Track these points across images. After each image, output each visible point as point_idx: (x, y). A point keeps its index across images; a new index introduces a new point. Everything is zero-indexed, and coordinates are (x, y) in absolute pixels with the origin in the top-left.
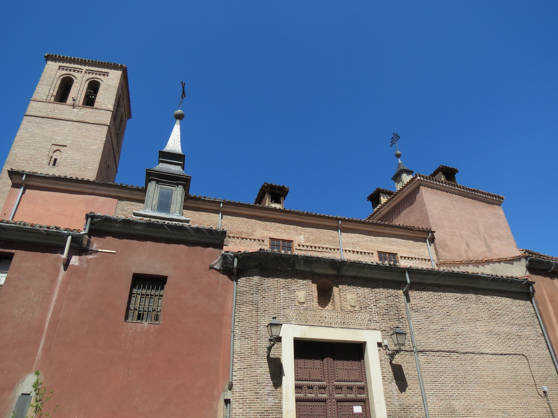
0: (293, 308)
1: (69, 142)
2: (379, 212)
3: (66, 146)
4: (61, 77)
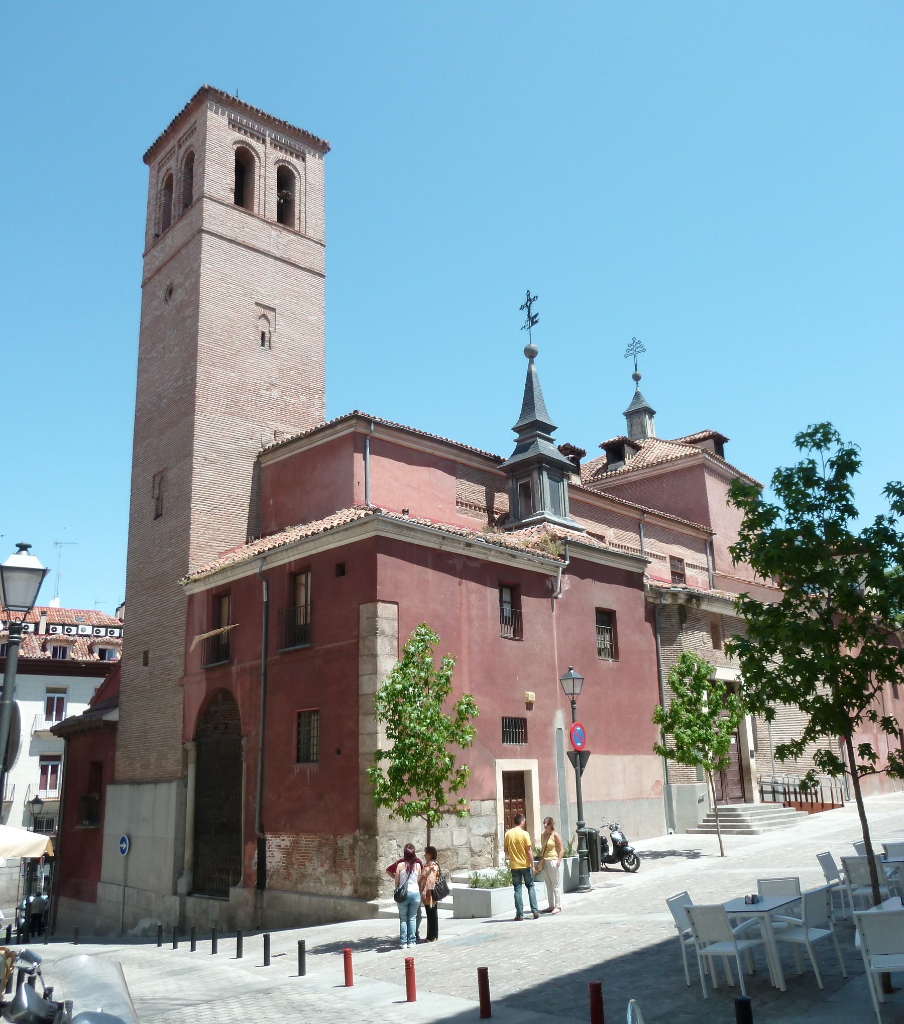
1: (277, 301)
2: (625, 476)
4: (235, 147)
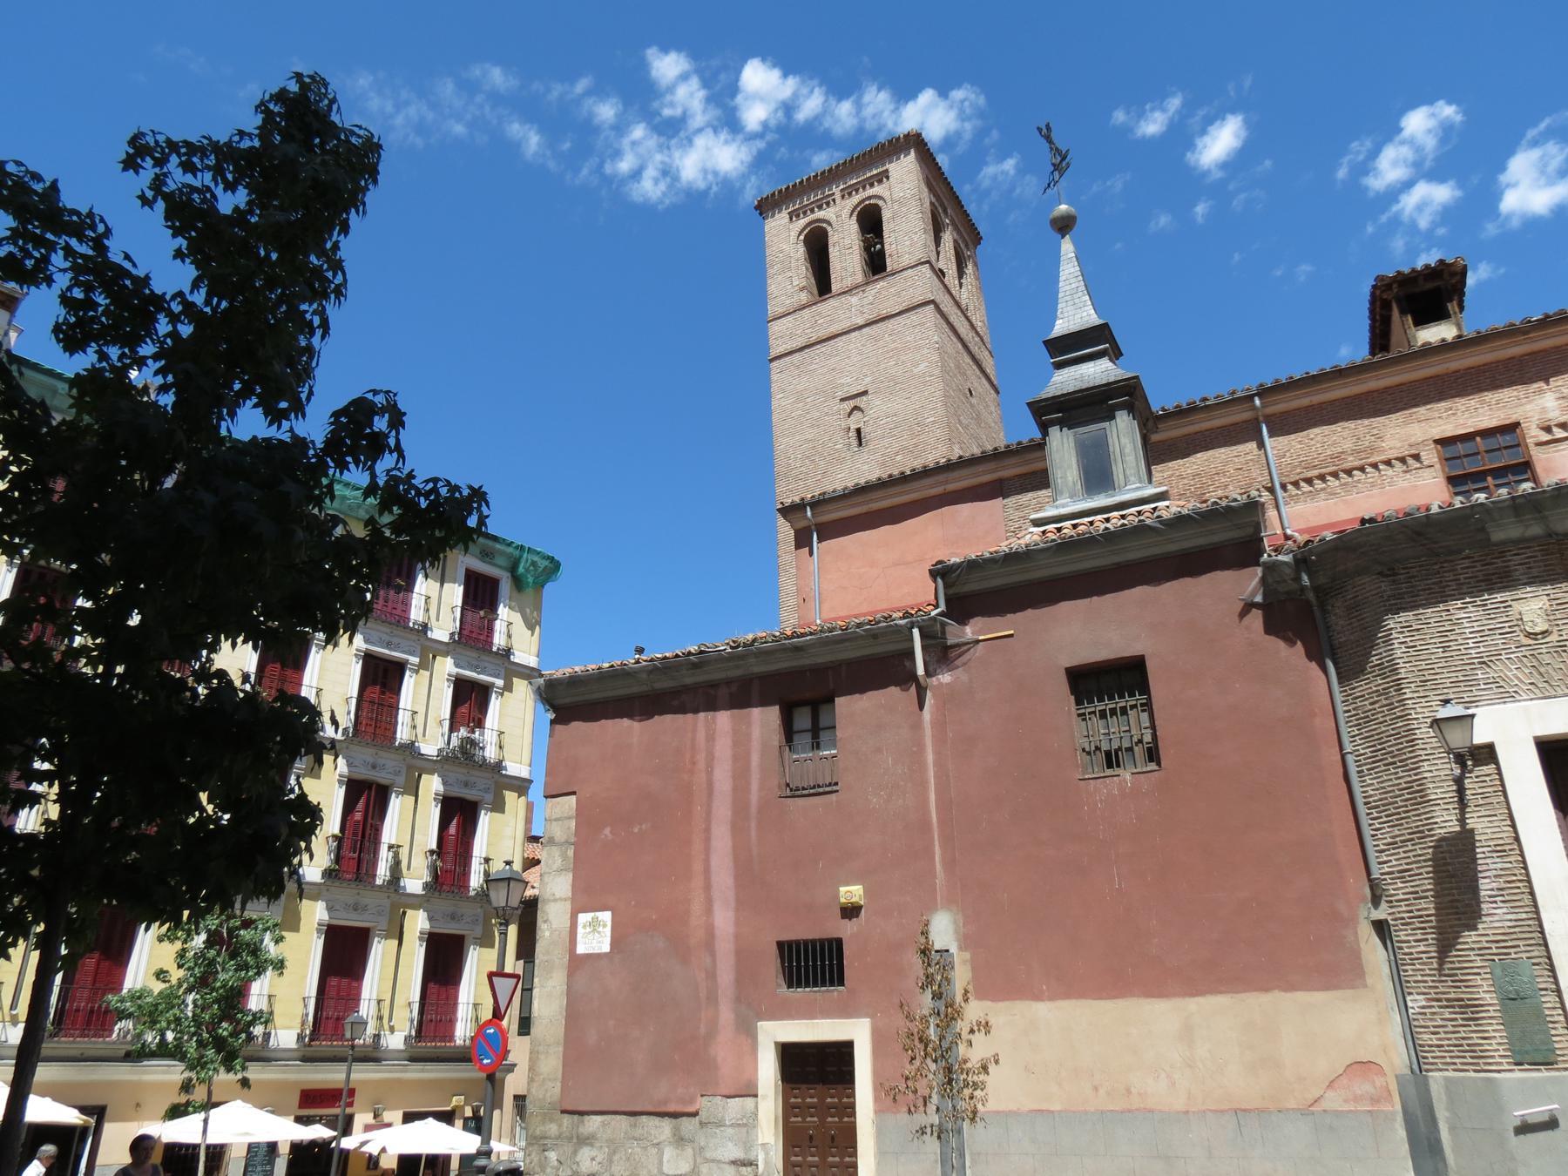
0: (1512, 656)
1: (868, 380)
3: (865, 393)
4: (802, 237)
